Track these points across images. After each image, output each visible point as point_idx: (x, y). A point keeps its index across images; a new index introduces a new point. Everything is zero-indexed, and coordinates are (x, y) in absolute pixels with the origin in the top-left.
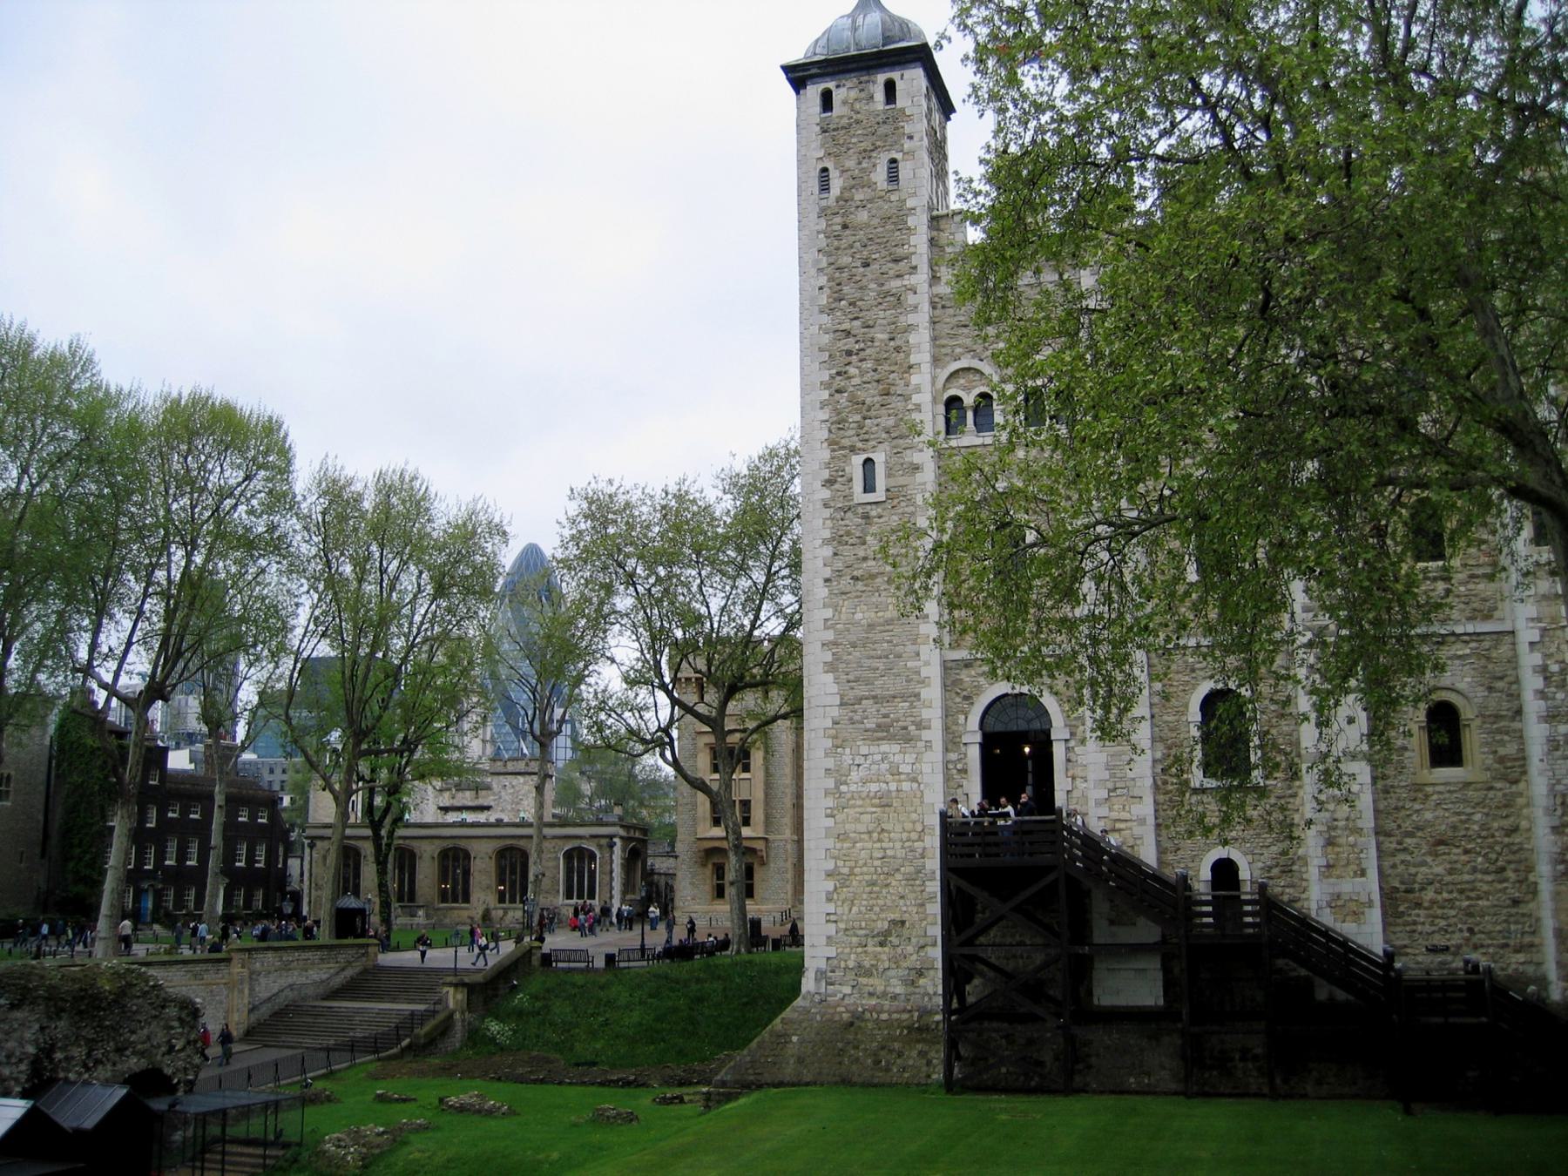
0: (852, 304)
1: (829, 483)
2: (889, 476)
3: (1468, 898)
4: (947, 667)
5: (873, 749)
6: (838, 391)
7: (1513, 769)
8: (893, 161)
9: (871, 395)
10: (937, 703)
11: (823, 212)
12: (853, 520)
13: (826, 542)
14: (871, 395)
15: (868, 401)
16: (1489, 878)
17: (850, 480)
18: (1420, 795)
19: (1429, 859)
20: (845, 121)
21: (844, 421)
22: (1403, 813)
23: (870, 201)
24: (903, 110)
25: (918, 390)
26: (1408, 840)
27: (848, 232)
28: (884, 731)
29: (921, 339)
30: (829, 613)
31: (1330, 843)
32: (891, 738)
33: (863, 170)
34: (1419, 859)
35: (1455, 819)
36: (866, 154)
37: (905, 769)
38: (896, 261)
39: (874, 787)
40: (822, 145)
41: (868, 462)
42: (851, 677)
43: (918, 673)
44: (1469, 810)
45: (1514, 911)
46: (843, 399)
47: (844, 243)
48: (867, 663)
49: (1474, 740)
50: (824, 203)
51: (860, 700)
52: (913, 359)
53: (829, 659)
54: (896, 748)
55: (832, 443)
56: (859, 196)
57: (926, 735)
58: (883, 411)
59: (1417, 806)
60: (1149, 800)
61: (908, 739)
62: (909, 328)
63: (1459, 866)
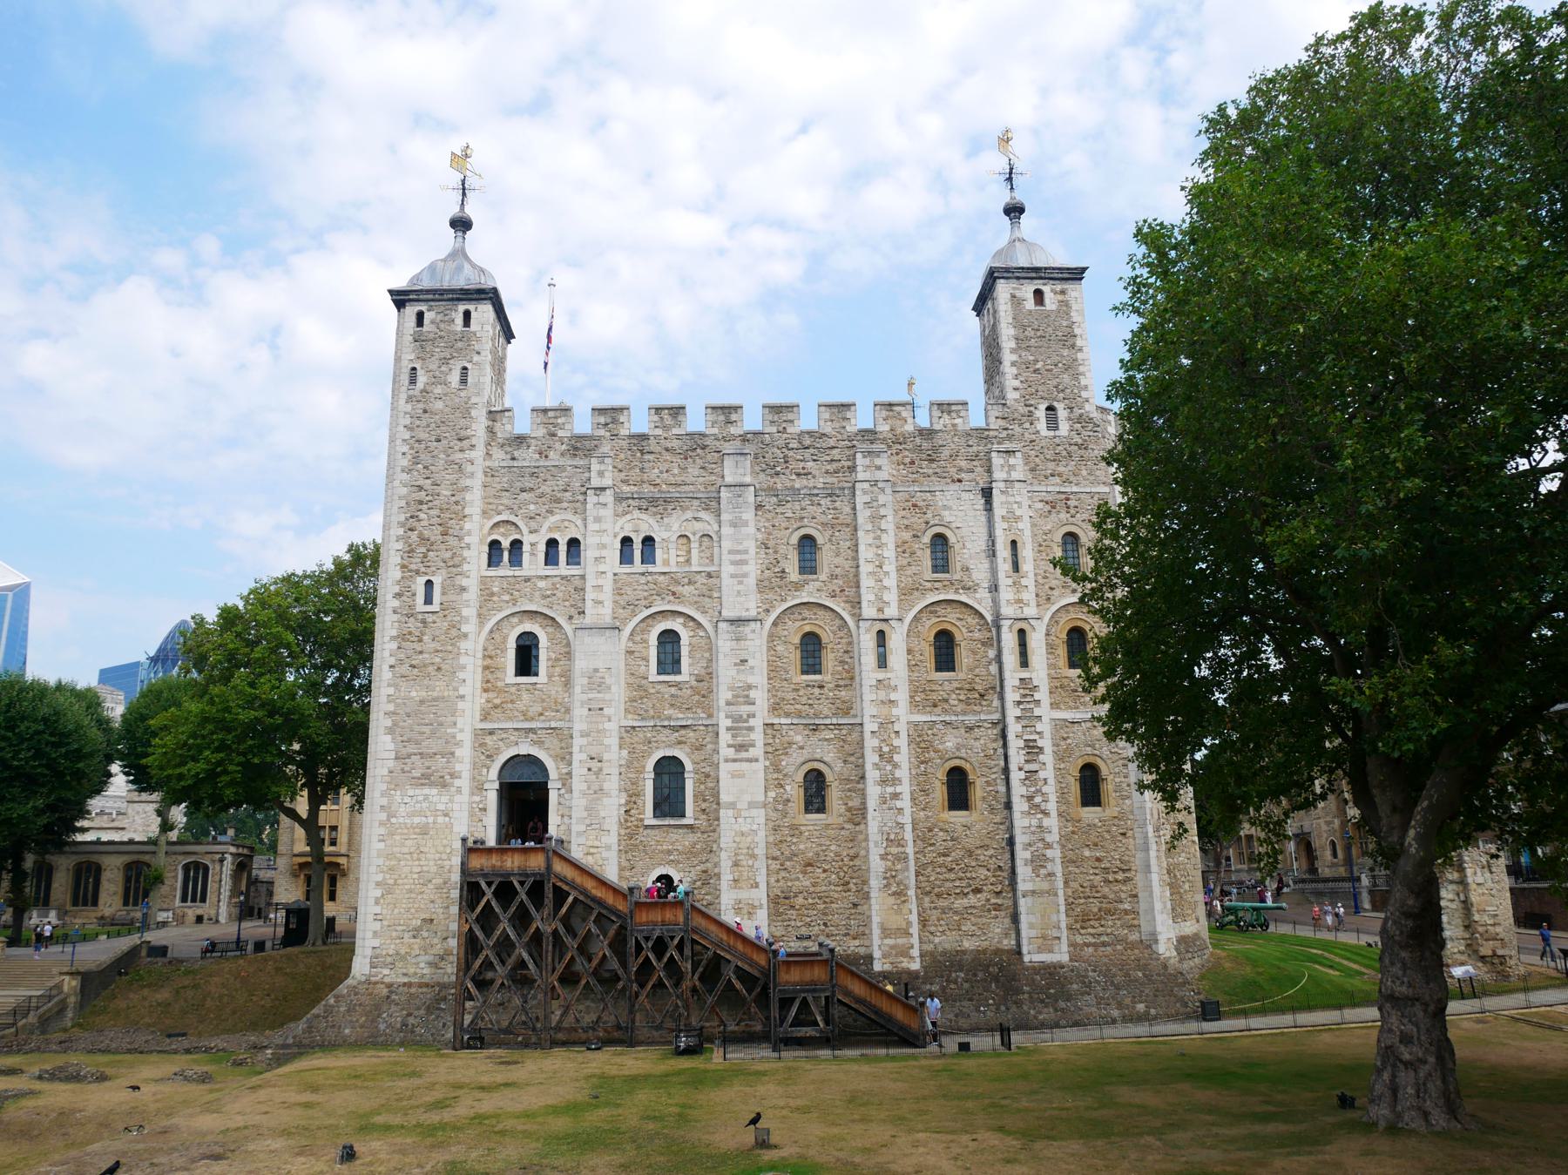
1: (398, 595)
2: (443, 594)
7: (858, 815)
9: (434, 534)
13: (393, 638)
14: (434, 534)
21: (412, 551)
41: (429, 583)
46: (414, 536)
49: (834, 795)
55: (403, 566)
58: (443, 547)
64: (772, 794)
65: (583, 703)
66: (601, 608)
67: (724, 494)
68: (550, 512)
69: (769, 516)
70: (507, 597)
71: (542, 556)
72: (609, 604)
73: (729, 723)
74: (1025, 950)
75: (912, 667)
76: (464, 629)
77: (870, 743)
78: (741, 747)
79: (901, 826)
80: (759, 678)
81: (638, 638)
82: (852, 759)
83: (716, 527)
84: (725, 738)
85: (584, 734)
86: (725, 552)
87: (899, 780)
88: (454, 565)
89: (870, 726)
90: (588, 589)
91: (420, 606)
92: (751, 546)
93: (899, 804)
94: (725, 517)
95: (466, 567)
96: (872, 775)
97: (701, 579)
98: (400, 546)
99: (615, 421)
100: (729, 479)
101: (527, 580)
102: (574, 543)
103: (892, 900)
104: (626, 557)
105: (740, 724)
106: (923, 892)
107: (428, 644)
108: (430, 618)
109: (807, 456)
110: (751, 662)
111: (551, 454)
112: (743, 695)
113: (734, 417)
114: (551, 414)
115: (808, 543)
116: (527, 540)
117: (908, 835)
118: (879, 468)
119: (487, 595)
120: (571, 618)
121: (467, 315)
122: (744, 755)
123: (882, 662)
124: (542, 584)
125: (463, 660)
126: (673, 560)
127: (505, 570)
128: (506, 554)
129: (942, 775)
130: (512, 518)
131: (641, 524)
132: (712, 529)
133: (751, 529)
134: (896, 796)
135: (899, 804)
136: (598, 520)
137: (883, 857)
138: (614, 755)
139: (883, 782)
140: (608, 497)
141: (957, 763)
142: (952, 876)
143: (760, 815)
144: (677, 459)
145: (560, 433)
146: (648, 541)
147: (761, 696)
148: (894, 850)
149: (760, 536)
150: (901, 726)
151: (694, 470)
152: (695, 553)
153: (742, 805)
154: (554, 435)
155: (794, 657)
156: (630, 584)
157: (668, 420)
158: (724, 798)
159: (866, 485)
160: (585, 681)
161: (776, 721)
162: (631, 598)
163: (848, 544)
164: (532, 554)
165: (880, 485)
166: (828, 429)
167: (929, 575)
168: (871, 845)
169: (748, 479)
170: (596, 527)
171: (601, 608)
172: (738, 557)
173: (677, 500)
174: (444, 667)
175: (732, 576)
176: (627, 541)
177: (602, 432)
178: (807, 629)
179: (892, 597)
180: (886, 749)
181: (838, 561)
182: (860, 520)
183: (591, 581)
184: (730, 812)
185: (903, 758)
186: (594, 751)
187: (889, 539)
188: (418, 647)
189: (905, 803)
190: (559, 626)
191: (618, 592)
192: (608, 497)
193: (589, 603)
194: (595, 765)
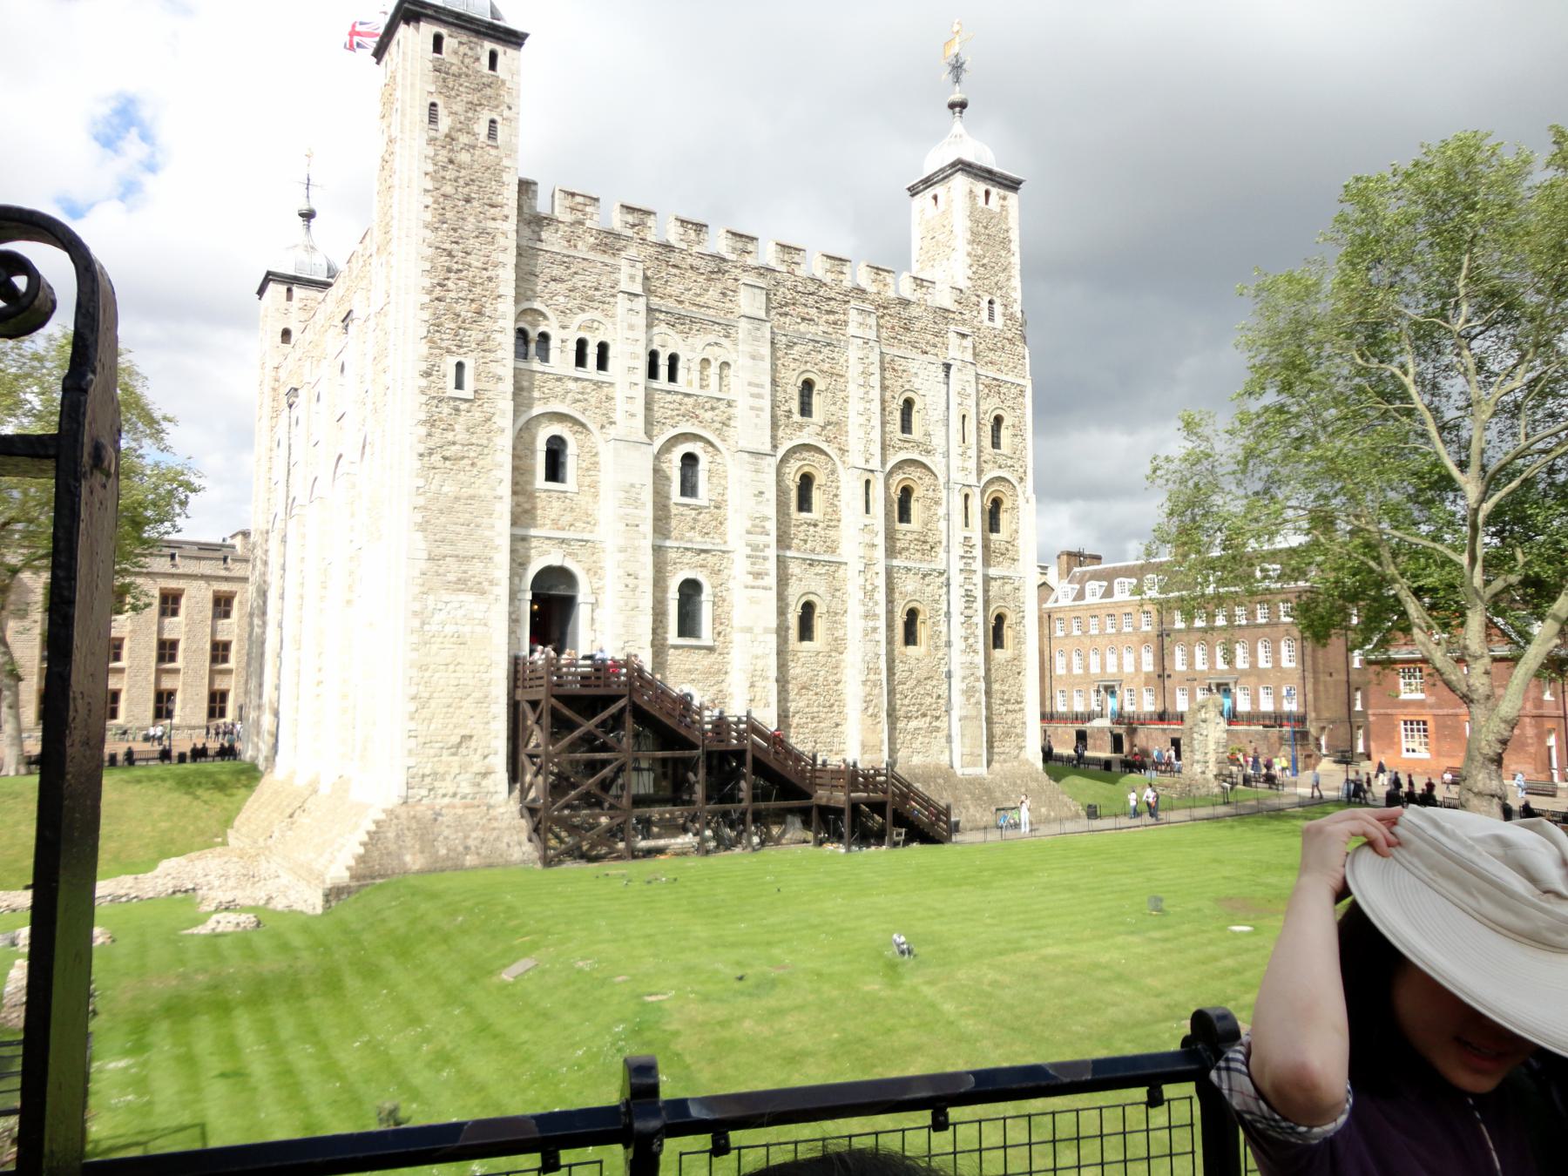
0: (455, 230)
4: (515, 539)
5: (454, 597)
6: (438, 299)
8: (493, 122)
12: (446, 409)
14: (465, 310)
20: (454, 69)
23: (474, 147)
24: (503, 82)
30: (421, 483)
31: (752, 685)
33: (469, 119)
36: (473, 106)
38: (492, 206)
41: (460, 366)
47: (448, 175)
48: (451, 528)
50: (433, 133)
52: (501, 291)
55: (432, 341)
61: (483, 593)
68: (583, 310)
73: (748, 551)
74: (957, 765)
75: (888, 514)
78: (758, 575)
79: (878, 656)
80: (771, 510)
83: (734, 356)
85: (623, 550)
88: (484, 346)
93: (876, 637)
95: (500, 354)
97: (722, 406)
99: (642, 224)
101: (559, 380)
102: (603, 348)
103: (870, 721)
104: (653, 373)
105: (755, 553)
106: (889, 715)
107: (460, 434)
108: (464, 406)
110: (766, 495)
111: (580, 244)
112: (757, 528)
113: (750, 247)
114: (579, 199)
115: (808, 386)
119: (518, 390)
120: (602, 427)
121: (493, 57)
122: (759, 582)
123: (867, 511)
124: (571, 385)
126: (696, 383)
127: (536, 365)
131: (668, 341)
133: (767, 364)
134: (875, 630)
135: (876, 637)
136: (631, 327)
137: (864, 683)
138: (648, 573)
142: (906, 702)
143: (772, 640)
144: (701, 279)
146: (673, 360)
147: (772, 526)
148: (872, 677)
151: (713, 294)
152: (713, 380)
154: (582, 223)
155: (794, 495)
157: (692, 235)
160: (623, 495)
161: (781, 553)
163: (842, 394)
166: (828, 279)
167: (900, 435)
169: (762, 315)
170: (630, 334)
173: (702, 321)
174: (480, 463)
175: (752, 408)
176: (653, 356)
177: (629, 232)
178: (806, 469)
179: (876, 448)
181: (833, 408)
185: (881, 596)
187: (875, 394)
188: (450, 436)
192: (640, 304)
194: (630, 581)
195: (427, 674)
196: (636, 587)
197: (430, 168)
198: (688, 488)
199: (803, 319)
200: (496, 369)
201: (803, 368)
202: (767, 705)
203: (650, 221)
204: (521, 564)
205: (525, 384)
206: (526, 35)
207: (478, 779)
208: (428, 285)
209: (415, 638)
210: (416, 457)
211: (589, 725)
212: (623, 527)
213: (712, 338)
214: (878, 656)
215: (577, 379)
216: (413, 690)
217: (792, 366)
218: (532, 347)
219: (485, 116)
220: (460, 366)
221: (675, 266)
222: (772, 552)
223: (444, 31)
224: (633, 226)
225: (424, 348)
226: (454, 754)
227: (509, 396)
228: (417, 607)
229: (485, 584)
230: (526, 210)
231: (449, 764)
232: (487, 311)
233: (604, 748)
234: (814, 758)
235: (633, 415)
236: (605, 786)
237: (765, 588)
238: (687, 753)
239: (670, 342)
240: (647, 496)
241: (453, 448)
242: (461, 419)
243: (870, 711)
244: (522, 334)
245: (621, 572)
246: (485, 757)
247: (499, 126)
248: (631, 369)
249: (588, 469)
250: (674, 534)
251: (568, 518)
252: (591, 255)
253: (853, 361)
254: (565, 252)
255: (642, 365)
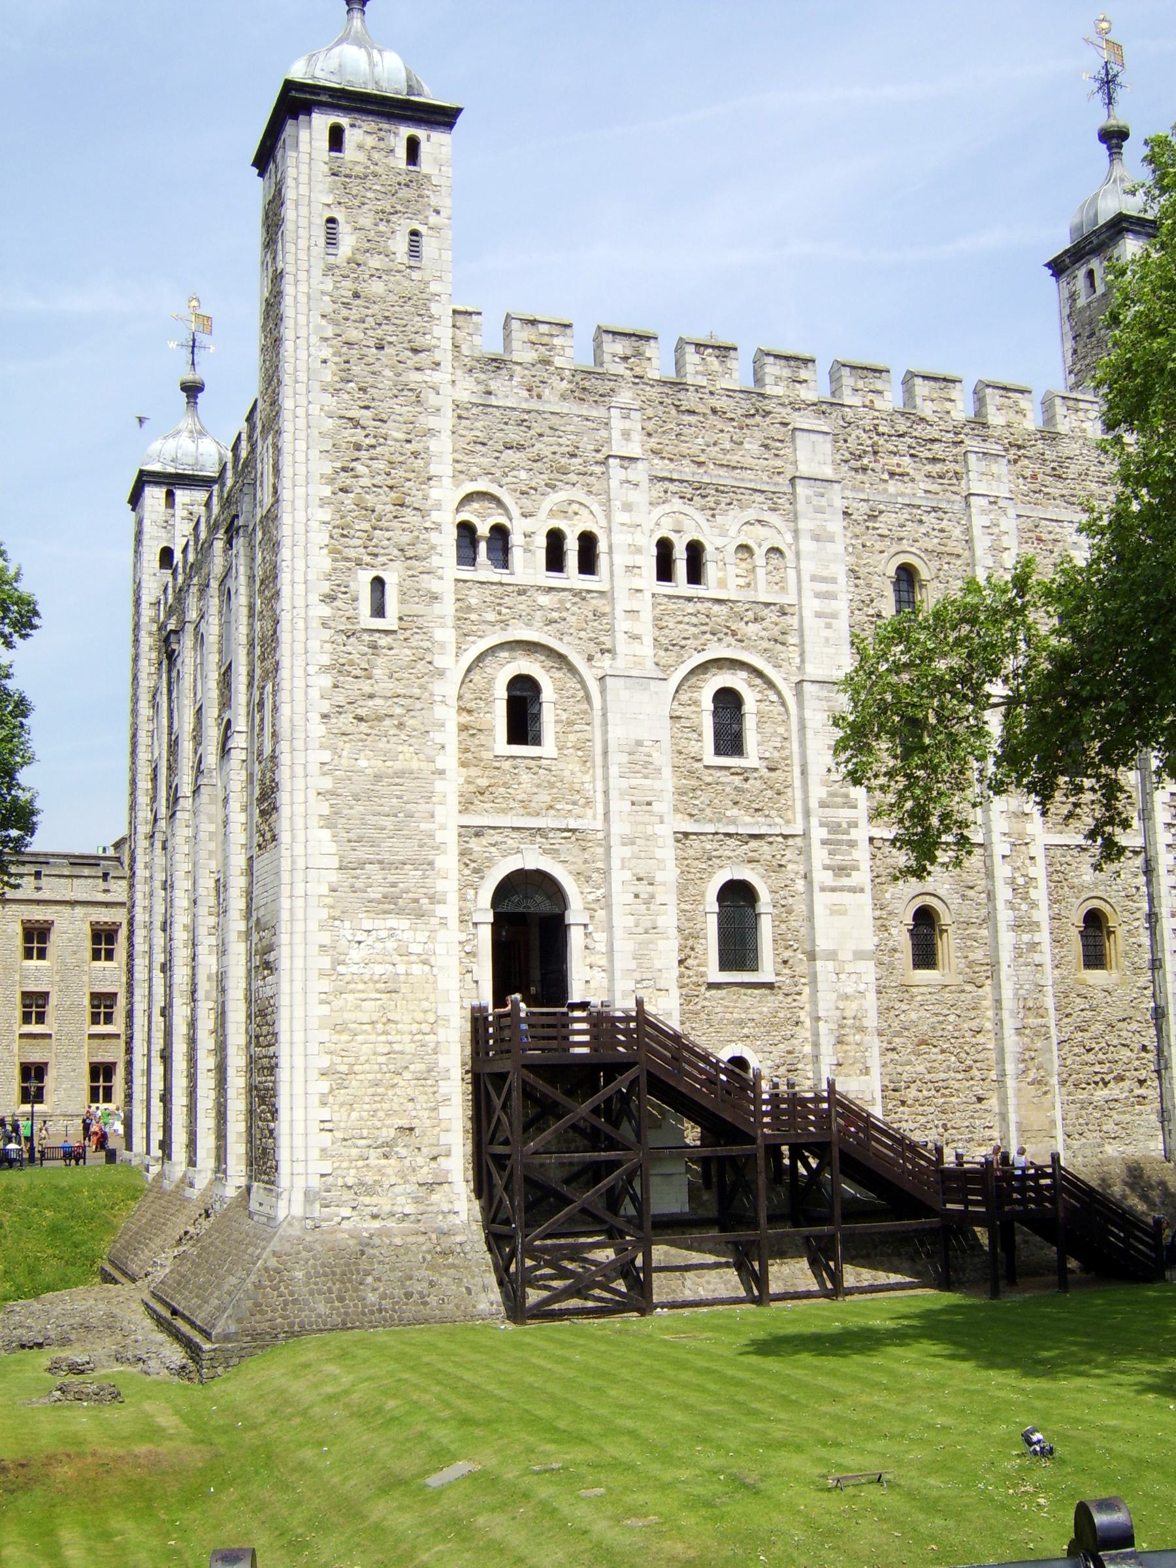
0: (363, 390)
2: (402, 602)
3: (944, 1095)
5: (379, 923)
6: (341, 490)
8: (414, 233)
9: (382, 502)
10: (454, 875)
11: (330, 269)
14: (382, 502)
15: (379, 508)
16: (959, 1076)
17: (355, 600)
18: (906, 996)
19: (913, 1058)
22: (893, 1012)
23: (388, 272)
24: (427, 177)
25: (438, 506)
26: (897, 1040)
27: (358, 302)
28: (392, 904)
29: (442, 448)
30: (326, 756)
32: (400, 912)
33: (380, 234)
34: (905, 1058)
35: (935, 1019)
36: (384, 216)
37: (416, 948)
38: (415, 351)
39: (379, 969)
40: (331, 191)
42: (352, 836)
43: (432, 836)
44: (946, 1012)
45: (978, 1106)
51: (362, 864)
52: (433, 470)
53: (325, 809)
54: (404, 923)
56: (375, 262)
57: (440, 910)
58: (395, 524)
59: (904, 1007)
60: (675, 992)
62: (430, 432)
63: (936, 1065)
64: (876, 940)
65: (622, 794)
66: (635, 648)
67: (802, 488)
69: (858, 530)
70: (491, 616)
71: (541, 556)
72: (648, 640)
73: (823, 833)
76: (440, 661)
77: (1002, 871)
78: (841, 870)
81: (684, 697)
82: (971, 893)
83: (789, 538)
84: (820, 855)
85: (629, 841)
86: (805, 577)
87: (1037, 924)
89: (1000, 847)
90: (619, 613)
91: (366, 619)
92: (839, 571)
93: (1037, 958)
94: (803, 524)
95: (435, 561)
96: (1004, 916)
97: (771, 615)
98: (326, 514)
99: (638, 354)
100: (804, 469)
101: (522, 592)
102: (588, 542)
104: (665, 572)
108: (384, 641)
109: (903, 448)
111: (547, 393)
113: (803, 374)
114: (543, 328)
116: (517, 530)
117: (1049, 1002)
118: (999, 479)
119: (464, 610)
120: (590, 658)
122: (845, 881)
124: (544, 600)
125: (440, 712)
126: (733, 582)
128: (483, 547)
129: (1077, 918)
130: (494, 489)
131: (687, 524)
132: (784, 541)
133: (838, 547)
136: (628, 507)
137: (1019, 1031)
138: (669, 874)
139: (1017, 926)
140: (639, 473)
141: (1096, 904)
142: (1090, 1057)
143: (869, 971)
145: (558, 362)
146: (695, 551)
148: (1032, 1021)
149: (851, 560)
150: (1037, 850)
151: (752, 446)
152: (760, 572)
153: (845, 955)
154: (546, 362)
156: (673, 614)
157: (714, 363)
158: (823, 943)
159: (984, 502)
160: (624, 758)
161: (877, 833)
162: (674, 634)
164: (527, 550)
165: (1001, 503)
166: (926, 409)
168: (1006, 1015)
169: (828, 472)
170: (624, 517)
171: (635, 648)
172: (823, 587)
175: (818, 615)
176: (664, 548)
177: (620, 369)
180: (1020, 881)
182: (979, 553)
183: (623, 602)
184: (830, 965)
185: (1040, 894)
186: (642, 869)
189: (1045, 956)
190: (573, 670)
191: (658, 623)
193: (621, 638)
194: (643, 888)
195: (345, 1037)
196: (652, 897)
197: (329, 308)
198: (729, 740)
199: (892, 474)
200: (431, 584)
201: (895, 548)
202: (866, 1071)
203: (650, 350)
204: (476, 871)
205: (474, 601)
206: (457, 111)
207: (422, 1192)
208: (329, 471)
209: (325, 985)
210: (318, 718)
211: (584, 1108)
212: (627, 806)
213: (751, 514)
214: (1040, 988)
215: (551, 589)
216: (325, 1062)
217: (879, 546)
218: (483, 547)
219: (404, 226)
220: (378, 584)
221: (691, 412)
222: (861, 834)
223: (344, 121)
224: (625, 359)
225: (324, 562)
226: (386, 1156)
227: (450, 621)
228: (325, 938)
229: (424, 901)
230: (465, 350)
231: (380, 1170)
232: (415, 500)
233: (613, 1145)
234: (939, 1150)
235: (636, 637)
236: (613, 1200)
237: (852, 890)
238: (735, 1150)
239: (688, 524)
240: (663, 759)
241: (370, 703)
242: (380, 661)
243: (1032, 1074)
244: (466, 531)
245: (627, 875)
246: (434, 1158)
247: (424, 241)
248: (630, 569)
249: (570, 723)
250: (708, 810)
251: (545, 797)
252: (564, 407)
253: (977, 532)
254: (525, 406)
255: (649, 562)
